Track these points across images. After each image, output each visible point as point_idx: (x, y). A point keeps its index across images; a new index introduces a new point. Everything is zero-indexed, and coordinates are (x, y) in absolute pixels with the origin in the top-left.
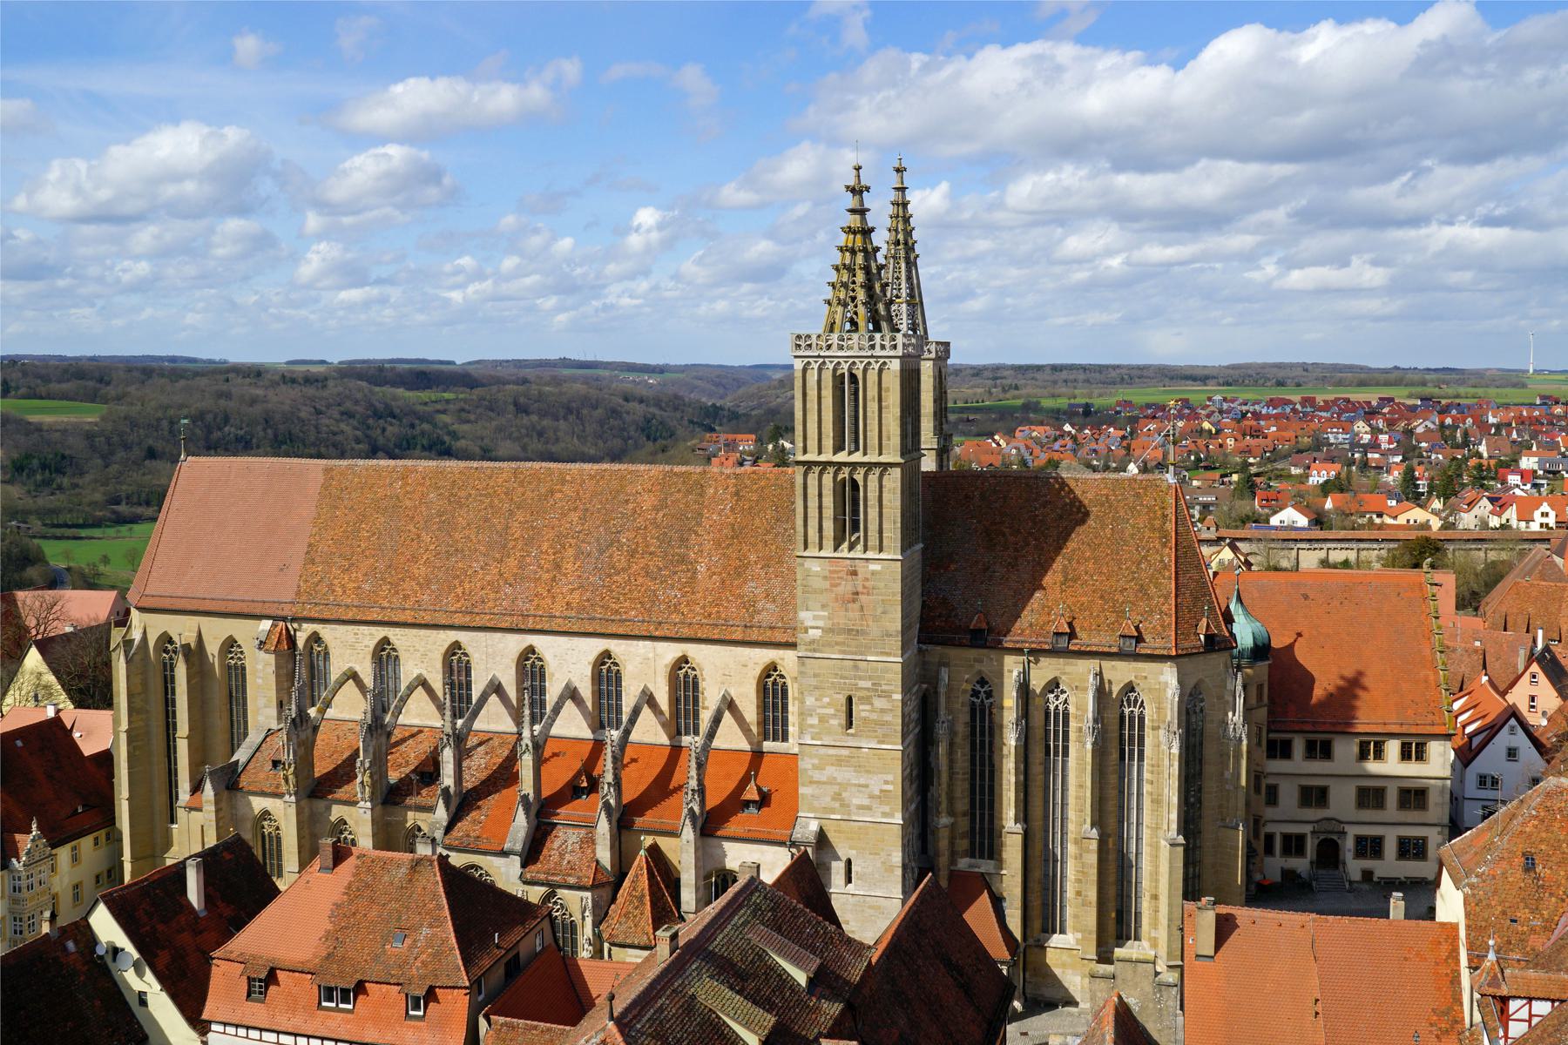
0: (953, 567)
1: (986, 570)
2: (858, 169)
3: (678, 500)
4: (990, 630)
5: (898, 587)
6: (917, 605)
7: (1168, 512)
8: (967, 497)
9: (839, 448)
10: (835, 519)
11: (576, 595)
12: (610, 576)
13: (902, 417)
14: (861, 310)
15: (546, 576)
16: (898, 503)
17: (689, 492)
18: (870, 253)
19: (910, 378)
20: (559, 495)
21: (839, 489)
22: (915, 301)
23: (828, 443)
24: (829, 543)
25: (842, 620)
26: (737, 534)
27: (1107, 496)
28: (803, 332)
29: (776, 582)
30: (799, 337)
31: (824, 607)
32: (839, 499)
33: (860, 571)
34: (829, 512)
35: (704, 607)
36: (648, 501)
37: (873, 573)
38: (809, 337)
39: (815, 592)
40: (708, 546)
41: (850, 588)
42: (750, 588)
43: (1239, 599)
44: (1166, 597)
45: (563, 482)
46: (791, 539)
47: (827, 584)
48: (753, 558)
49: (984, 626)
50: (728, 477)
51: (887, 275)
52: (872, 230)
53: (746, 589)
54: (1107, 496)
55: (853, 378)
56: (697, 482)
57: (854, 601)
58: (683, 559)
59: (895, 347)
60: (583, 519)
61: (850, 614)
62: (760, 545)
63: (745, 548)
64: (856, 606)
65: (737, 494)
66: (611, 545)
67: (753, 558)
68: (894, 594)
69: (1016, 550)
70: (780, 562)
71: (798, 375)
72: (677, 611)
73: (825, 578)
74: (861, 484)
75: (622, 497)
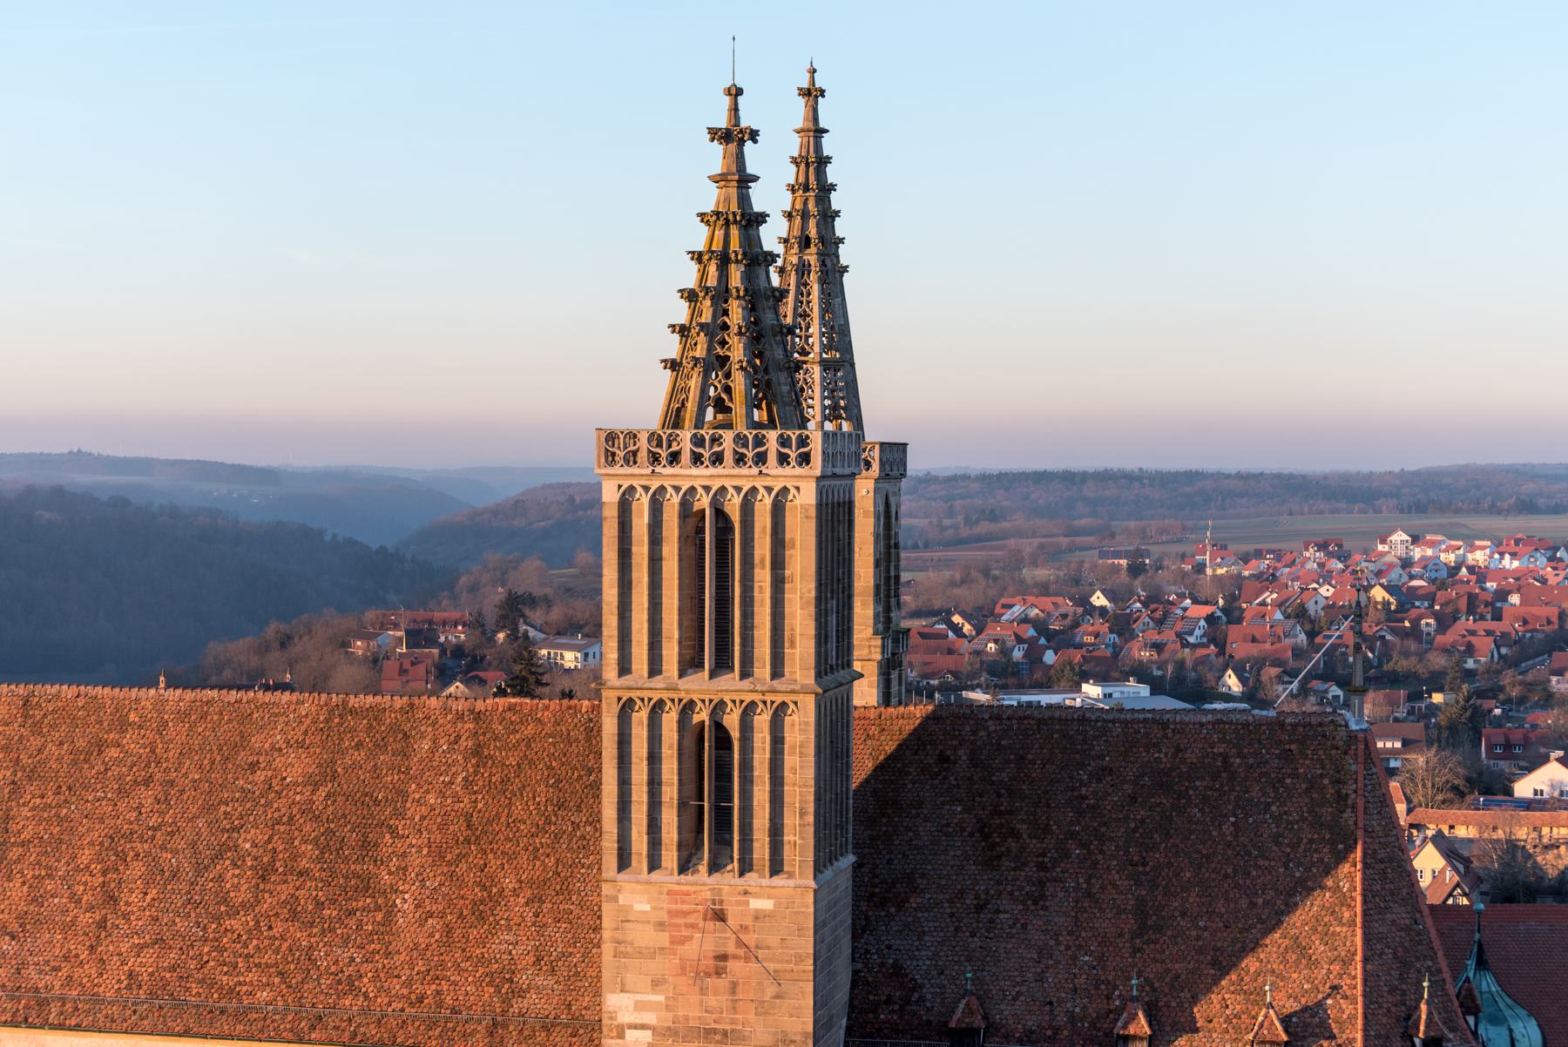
0: (914, 901)
1: (980, 908)
2: (735, 93)
3: (356, 766)
4: (991, 1028)
5: (807, 945)
6: (844, 978)
7: (1349, 788)
8: (943, 759)
9: (690, 663)
10: (682, 805)
11: (148, 956)
12: (217, 919)
13: (819, 600)
14: (739, 382)
15: (86, 919)
16: (810, 773)
17: (380, 747)
18: (758, 260)
19: (834, 517)
20: (114, 753)
21: (690, 743)
22: (840, 364)
23: (671, 653)
24: (670, 857)
25: (691, 1011)
26: (476, 833)
27: (1225, 757)
28: (620, 424)
29: (558, 935)
30: (611, 437)
31: (656, 984)
32: (690, 765)
33: (732, 912)
34: (670, 793)
35: (409, 983)
36: (296, 767)
37: (758, 916)
38: (633, 436)
39: (640, 953)
40: (415, 861)
41: (710, 947)
42: (509, 944)
43: (1482, 964)
44: (1347, 962)
45: (123, 725)
46: (589, 847)
47: (663, 939)
48: (509, 883)
49: (978, 1022)
50: (460, 717)
51: (788, 308)
52: (761, 218)
53: (499, 944)
54: (1225, 757)
55: (720, 514)
56: (394, 728)
57: (719, 973)
58: (366, 885)
59: (805, 459)
60: (163, 801)
61: (712, 1001)
62: (524, 858)
63: (494, 863)
64: (722, 983)
65: (477, 751)
66: (219, 856)
67: (509, 883)
68: (799, 959)
69: (1041, 867)
70: (565, 891)
71: (611, 513)
72: (352, 986)
73: (661, 926)
74: (735, 734)
75: (243, 757)
